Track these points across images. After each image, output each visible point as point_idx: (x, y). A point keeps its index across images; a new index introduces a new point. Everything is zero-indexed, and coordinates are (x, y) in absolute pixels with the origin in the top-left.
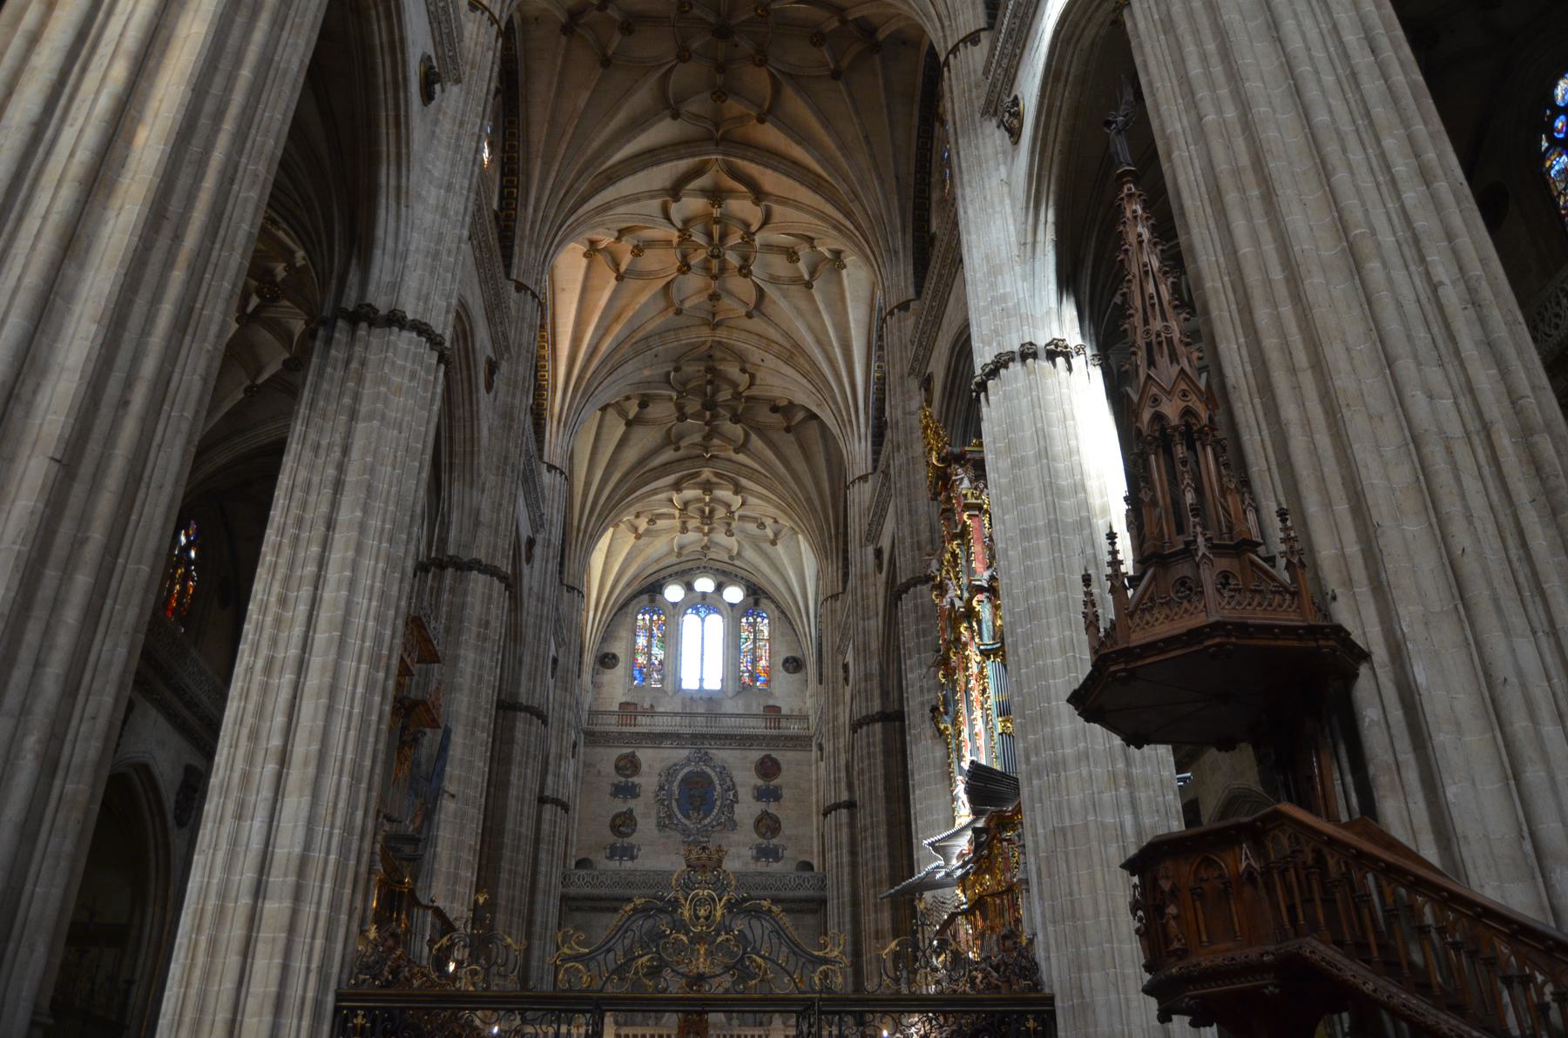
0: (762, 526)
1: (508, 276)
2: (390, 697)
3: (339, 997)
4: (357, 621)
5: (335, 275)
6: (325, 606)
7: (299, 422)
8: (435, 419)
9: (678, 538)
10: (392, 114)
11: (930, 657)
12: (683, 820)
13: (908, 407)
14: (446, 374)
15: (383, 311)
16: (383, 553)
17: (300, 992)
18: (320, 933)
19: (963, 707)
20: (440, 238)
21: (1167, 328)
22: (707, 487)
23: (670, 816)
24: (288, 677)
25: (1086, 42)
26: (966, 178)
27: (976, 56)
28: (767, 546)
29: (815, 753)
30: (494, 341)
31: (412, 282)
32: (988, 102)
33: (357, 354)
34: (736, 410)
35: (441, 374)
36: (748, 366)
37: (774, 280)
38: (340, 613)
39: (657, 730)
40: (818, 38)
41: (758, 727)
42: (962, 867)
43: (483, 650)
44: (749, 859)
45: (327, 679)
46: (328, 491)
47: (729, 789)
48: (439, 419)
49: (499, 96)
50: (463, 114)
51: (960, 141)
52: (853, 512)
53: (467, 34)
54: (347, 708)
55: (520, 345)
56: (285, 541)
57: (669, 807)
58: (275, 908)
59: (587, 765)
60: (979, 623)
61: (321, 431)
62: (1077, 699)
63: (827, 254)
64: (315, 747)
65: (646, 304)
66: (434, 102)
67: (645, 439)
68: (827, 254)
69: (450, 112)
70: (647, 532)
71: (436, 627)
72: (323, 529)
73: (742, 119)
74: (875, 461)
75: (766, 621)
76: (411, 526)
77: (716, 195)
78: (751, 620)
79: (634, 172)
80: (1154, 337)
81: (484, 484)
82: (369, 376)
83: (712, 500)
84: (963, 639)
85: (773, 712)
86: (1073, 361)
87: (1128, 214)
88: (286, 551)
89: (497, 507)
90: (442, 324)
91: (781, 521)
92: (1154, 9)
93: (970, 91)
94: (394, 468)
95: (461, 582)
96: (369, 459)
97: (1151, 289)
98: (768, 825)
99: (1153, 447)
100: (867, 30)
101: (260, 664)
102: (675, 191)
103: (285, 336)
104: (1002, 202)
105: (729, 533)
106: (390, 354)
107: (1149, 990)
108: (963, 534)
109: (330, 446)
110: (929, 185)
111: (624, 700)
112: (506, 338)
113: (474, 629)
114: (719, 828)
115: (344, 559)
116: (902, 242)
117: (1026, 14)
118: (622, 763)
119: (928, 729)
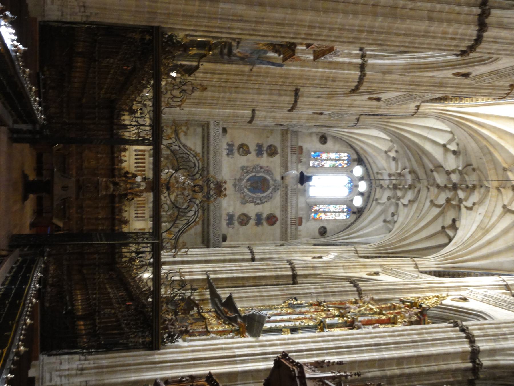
12: (246, 178)
23: (247, 172)
28: (382, 218)
34: (453, 200)
36: (476, 206)
44: (227, 211)
47: (261, 200)
57: (252, 171)
59: (272, 131)
70: (389, 156)
75: (345, 218)
81: (405, 75)
83: (406, 189)
89: (393, 82)
95: (355, 67)
98: (244, 220)
105: (389, 199)
111: (304, 147)
114: (242, 196)
118: (273, 148)
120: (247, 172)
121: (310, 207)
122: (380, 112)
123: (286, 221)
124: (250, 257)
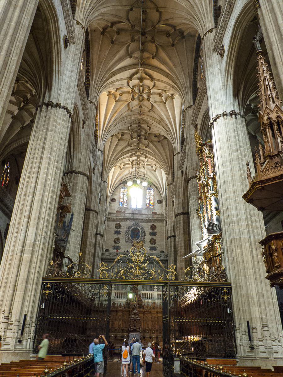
0: (152, 167)
1: (88, 99)
2: (57, 202)
3: (43, 279)
4: (48, 183)
5: (42, 94)
6: (40, 179)
7: (33, 132)
8: (69, 132)
9: (131, 170)
10: (56, 50)
11: (195, 197)
13: (191, 133)
14: (71, 121)
15: (55, 103)
16: (55, 165)
17: (33, 278)
18: (38, 263)
19: (205, 209)
20: (70, 85)
21: (272, 94)
22: (138, 156)
23: (129, 239)
24: (31, 197)
25: (243, 27)
26: (208, 69)
27: (211, 36)
28: (153, 172)
29: (165, 223)
30: (84, 115)
31: (63, 96)
32: (215, 48)
33: (48, 114)
35: (70, 120)
36: (149, 125)
37: (156, 102)
38: (44, 180)
39: (126, 218)
40: (168, 35)
41: (150, 217)
42: (204, 251)
43: (82, 194)
45: (41, 198)
46: (41, 149)
47: (143, 233)
48: (70, 132)
49: (85, 52)
50: (75, 52)
51: (207, 59)
52: (176, 162)
53: (76, 31)
54: (46, 205)
55: (91, 117)
56: (30, 162)
58: (26, 256)
59: (108, 226)
60: (210, 187)
61: (39, 134)
62: (245, 196)
63: (170, 95)
64: (37, 215)
65: (123, 108)
66: (67, 48)
67: (123, 144)
68: (170, 95)
69: (72, 52)
71: (70, 187)
72: (40, 159)
73: (148, 58)
74: (182, 149)
76: (62, 159)
77: (141, 79)
78: (149, 190)
79: (120, 73)
80: (268, 97)
81: (82, 152)
82: (51, 120)
83: (139, 160)
84: (206, 191)
85: (154, 214)
86: (237, 117)
87: (260, 63)
88: (30, 165)
90: (71, 107)
91: (157, 165)
92: (268, 6)
93: (210, 45)
94: (58, 144)
96: (51, 141)
97: (267, 83)
98: (153, 241)
99: (268, 126)
100: (182, 33)
101: (23, 193)
102: (131, 78)
103: (30, 114)
104: (218, 74)
105: (144, 168)
106: (57, 114)
107: (268, 278)
108: (206, 164)
109: (41, 138)
110: (197, 75)
112: (87, 115)
113: (80, 189)
115: (45, 167)
116: (190, 90)
117: (226, 21)
118: (117, 226)
119: (196, 215)
120: (129, 239)
121: (147, 208)
122: (100, 168)
123: (154, 220)
124: (172, 239)
